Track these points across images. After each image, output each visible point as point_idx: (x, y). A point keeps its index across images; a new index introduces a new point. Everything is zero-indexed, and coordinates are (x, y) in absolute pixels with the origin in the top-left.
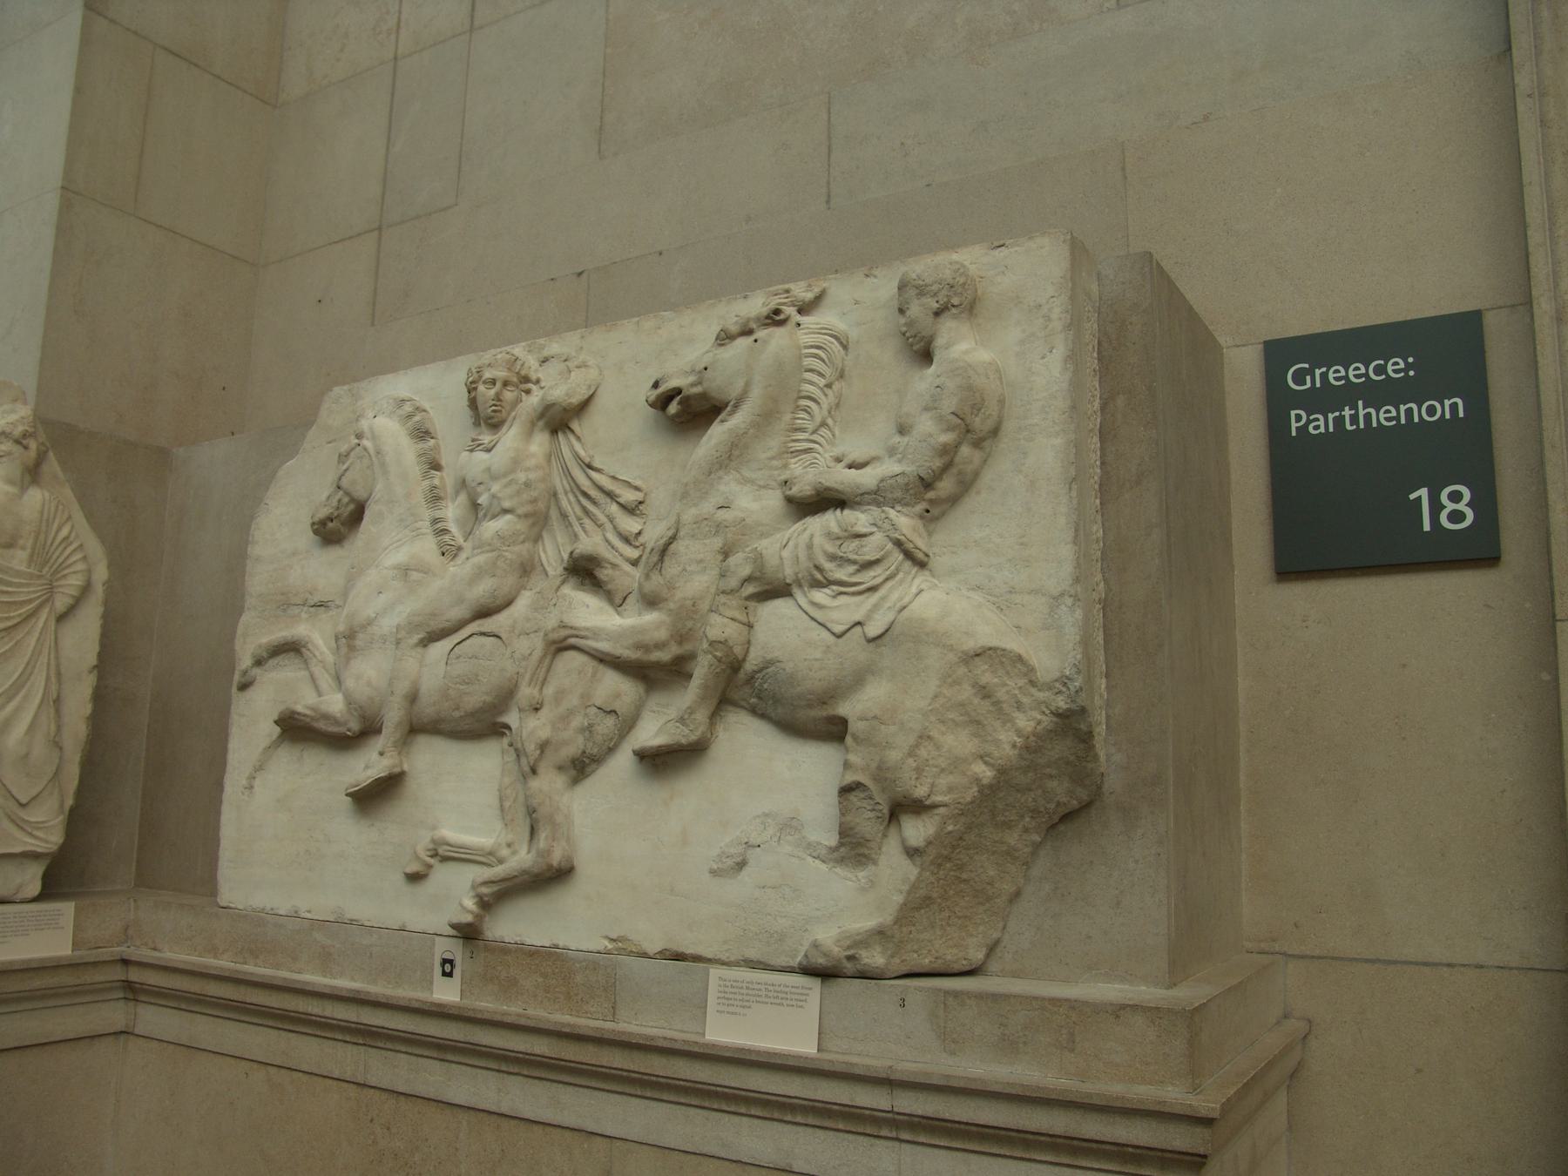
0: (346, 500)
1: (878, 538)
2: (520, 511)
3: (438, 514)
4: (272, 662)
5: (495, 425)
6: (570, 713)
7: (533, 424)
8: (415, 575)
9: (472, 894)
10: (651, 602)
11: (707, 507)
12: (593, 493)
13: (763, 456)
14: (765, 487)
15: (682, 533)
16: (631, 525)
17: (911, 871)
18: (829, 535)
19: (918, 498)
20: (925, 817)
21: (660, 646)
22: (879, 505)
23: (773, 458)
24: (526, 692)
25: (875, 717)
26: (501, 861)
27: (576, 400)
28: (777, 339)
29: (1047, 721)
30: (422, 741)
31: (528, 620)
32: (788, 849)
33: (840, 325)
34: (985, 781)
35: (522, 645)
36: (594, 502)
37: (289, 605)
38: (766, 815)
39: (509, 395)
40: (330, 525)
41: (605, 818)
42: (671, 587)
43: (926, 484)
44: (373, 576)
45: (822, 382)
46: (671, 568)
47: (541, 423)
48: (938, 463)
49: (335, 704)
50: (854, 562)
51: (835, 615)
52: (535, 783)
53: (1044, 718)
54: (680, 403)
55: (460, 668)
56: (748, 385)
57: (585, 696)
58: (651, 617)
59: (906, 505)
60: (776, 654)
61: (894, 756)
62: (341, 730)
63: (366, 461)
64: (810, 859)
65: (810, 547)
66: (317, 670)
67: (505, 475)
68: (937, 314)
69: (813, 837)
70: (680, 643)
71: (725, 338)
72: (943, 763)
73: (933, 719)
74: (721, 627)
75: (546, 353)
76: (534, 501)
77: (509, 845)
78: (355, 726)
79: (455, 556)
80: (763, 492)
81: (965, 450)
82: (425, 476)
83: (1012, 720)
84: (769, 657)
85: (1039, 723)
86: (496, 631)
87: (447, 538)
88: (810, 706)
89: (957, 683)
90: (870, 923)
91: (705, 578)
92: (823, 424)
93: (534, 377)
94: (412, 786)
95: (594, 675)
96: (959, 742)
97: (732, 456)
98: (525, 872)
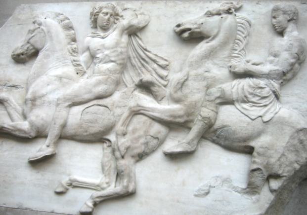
0: (31, 48)
1: (267, 89)
2: (118, 62)
3: (75, 58)
5: (105, 29)
6: (140, 137)
8: (65, 80)
9: (91, 201)
10: (177, 101)
11: (201, 71)
12: (147, 59)
13: (222, 56)
14: (223, 67)
15: (190, 79)
16: (164, 73)
19: (281, 78)
20: (278, 180)
21: (180, 117)
22: (268, 78)
23: (225, 58)
24: (119, 127)
25: (266, 147)
26: (103, 189)
27: (141, 25)
28: (229, 19)
31: (120, 102)
32: (225, 188)
33: (249, 18)
34: (297, 169)
35: (118, 111)
36: (147, 62)
38: (218, 177)
39: (112, 20)
40: (22, 56)
41: (151, 175)
42: (186, 96)
43: (284, 74)
44: (44, 78)
46: (186, 91)
48: (289, 68)
49: (25, 125)
50: (259, 96)
51: (251, 113)
52: (122, 162)
54: (189, 34)
55: (87, 117)
57: (146, 133)
58: (175, 107)
59: (277, 80)
60: (227, 124)
61: (273, 160)
63: (42, 34)
64: (234, 192)
65: (243, 89)
66: (12, 112)
67: (112, 48)
68: (289, 21)
69: (236, 185)
71: (210, 14)
72: (287, 163)
74: (206, 112)
75: (126, 6)
76: (123, 59)
77: (107, 183)
78: (33, 134)
79: (83, 75)
80: (222, 68)
81: (297, 65)
82: (69, 43)
84: (225, 124)
86: (106, 105)
87: (80, 68)
88: (240, 142)
89: (294, 138)
91: (199, 95)
92: (243, 49)
93: (121, 15)
94: (59, 158)
95: (150, 124)
96: (291, 157)
97: (210, 55)
98: (116, 193)
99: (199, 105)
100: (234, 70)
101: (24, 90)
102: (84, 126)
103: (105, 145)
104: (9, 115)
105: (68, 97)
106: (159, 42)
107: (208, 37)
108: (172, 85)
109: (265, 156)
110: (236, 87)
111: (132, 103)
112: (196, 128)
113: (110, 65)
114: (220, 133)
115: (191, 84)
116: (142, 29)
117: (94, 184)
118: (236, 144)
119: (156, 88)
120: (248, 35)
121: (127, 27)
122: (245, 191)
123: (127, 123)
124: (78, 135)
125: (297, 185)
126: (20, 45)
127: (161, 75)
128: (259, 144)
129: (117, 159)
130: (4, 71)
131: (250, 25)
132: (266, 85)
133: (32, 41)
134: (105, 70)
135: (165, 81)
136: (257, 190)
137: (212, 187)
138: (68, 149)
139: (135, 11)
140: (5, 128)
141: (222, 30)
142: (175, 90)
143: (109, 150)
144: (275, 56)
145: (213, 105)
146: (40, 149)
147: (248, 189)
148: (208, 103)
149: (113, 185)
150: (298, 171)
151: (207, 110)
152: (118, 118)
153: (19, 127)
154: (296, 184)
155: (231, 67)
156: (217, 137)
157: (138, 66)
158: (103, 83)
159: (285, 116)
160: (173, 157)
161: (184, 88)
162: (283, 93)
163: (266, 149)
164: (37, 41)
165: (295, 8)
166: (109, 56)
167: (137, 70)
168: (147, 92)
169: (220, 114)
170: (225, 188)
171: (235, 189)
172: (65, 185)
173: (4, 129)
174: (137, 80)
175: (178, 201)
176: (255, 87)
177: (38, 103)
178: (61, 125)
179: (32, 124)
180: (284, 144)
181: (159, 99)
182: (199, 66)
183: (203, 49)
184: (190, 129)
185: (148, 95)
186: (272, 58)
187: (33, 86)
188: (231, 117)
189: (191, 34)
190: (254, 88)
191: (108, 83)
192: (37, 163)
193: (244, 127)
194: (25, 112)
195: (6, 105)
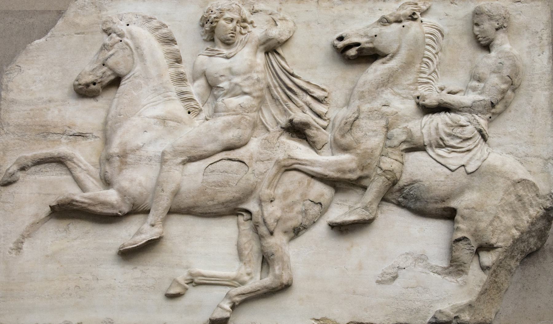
0: (109, 73)
1: (470, 128)
2: (255, 94)
3: (184, 89)
4: (33, 169)
7: (258, 48)
8: (171, 123)
10: (345, 149)
11: (376, 104)
13: (405, 83)
15: (362, 116)
16: (320, 108)
17: (484, 277)
18: (447, 124)
19: (488, 111)
20: (492, 252)
21: (350, 171)
22: (470, 112)
23: (410, 85)
25: (473, 208)
26: (243, 283)
27: (284, 38)
28: (414, 27)
29: (542, 212)
30: (175, 218)
31: (261, 154)
32: (420, 269)
34: (516, 237)
35: (260, 167)
37: (48, 134)
38: (408, 254)
40: (92, 87)
42: (358, 142)
43: (493, 105)
44: (136, 120)
45: (434, 52)
46: (358, 134)
47: (262, 47)
48: (499, 97)
49: (112, 196)
50: (460, 138)
51: (450, 161)
53: (540, 210)
54: (358, 50)
55: (214, 178)
56: (399, 47)
57: (304, 196)
58: (344, 157)
59: (483, 114)
60: (418, 178)
61: (483, 225)
62: (115, 211)
64: (432, 274)
65: (437, 129)
66: (82, 176)
67: (244, 73)
68: (497, 29)
69: (434, 263)
70: (362, 170)
71: (385, 21)
72: (502, 228)
73: (500, 209)
74: (388, 163)
75: (257, 8)
76: (261, 90)
77: (249, 274)
78: (126, 209)
79: (198, 114)
80: (405, 100)
81: (509, 92)
82: (171, 66)
83: (528, 211)
84: (414, 179)
85: (538, 213)
86: (240, 159)
87: (192, 103)
88: (436, 203)
89: (510, 194)
90: (465, 301)
91: (377, 139)
94: (167, 244)
95: (309, 184)
96: (508, 219)
97: (389, 81)
98: (266, 287)
99: (377, 153)
100: (423, 102)
101: (98, 143)
102: (209, 191)
103: (241, 219)
104: (77, 181)
105: (180, 149)
106: (309, 62)
108: (337, 124)
109: (472, 220)
111: (280, 155)
112: (376, 186)
113: (243, 100)
114: (409, 192)
115: (363, 124)
116: (283, 43)
117: (228, 277)
118: (432, 206)
119: (313, 132)
120: (441, 50)
121: (263, 41)
122: (447, 271)
124: (198, 207)
125: (518, 263)
126: (88, 68)
127: (318, 113)
128: (463, 204)
129: (261, 237)
130: (60, 111)
132: (469, 122)
134: (236, 107)
136: (463, 268)
137: (402, 269)
138: (180, 229)
139: (270, 14)
140: (77, 201)
141: (404, 45)
142: (342, 133)
143: (247, 227)
144: (479, 80)
146: (130, 233)
147: (451, 268)
148: (390, 150)
150: (518, 240)
151: (388, 160)
152: (261, 177)
153: (102, 198)
154: (517, 261)
155: (418, 97)
156: (404, 197)
157: (282, 98)
158: (234, 126)
159: (496, 164)
160: (342, 229)
161: (354, 129)
162: (490, 132)
163: (473, 210)
164: (118, 61)
165: (506, 11)
166: (241, 86)
167: (281, 104)
168: (299, 137)
169: (406, 164)
170: (420, 269)
171: (432, 268)
172: (183, 282)
173: (74, 203)
174: (283, 121)
175: (354, 293)
176: (453, 124)
177: (131, 160)
178: (172, 193)
179: (123, 193)
181: (319, 146)
182: (374, 99)
183: (378, 73)
184: (365, 188)
185: (301, 142)
186: (475, 83)
187: (119, 133)
188: (420, 168)
190: (452, 126)
191: (242, 127)
192: (128, 254)
193: (442, 181)
194: (109, 174)
195: (70, 167)
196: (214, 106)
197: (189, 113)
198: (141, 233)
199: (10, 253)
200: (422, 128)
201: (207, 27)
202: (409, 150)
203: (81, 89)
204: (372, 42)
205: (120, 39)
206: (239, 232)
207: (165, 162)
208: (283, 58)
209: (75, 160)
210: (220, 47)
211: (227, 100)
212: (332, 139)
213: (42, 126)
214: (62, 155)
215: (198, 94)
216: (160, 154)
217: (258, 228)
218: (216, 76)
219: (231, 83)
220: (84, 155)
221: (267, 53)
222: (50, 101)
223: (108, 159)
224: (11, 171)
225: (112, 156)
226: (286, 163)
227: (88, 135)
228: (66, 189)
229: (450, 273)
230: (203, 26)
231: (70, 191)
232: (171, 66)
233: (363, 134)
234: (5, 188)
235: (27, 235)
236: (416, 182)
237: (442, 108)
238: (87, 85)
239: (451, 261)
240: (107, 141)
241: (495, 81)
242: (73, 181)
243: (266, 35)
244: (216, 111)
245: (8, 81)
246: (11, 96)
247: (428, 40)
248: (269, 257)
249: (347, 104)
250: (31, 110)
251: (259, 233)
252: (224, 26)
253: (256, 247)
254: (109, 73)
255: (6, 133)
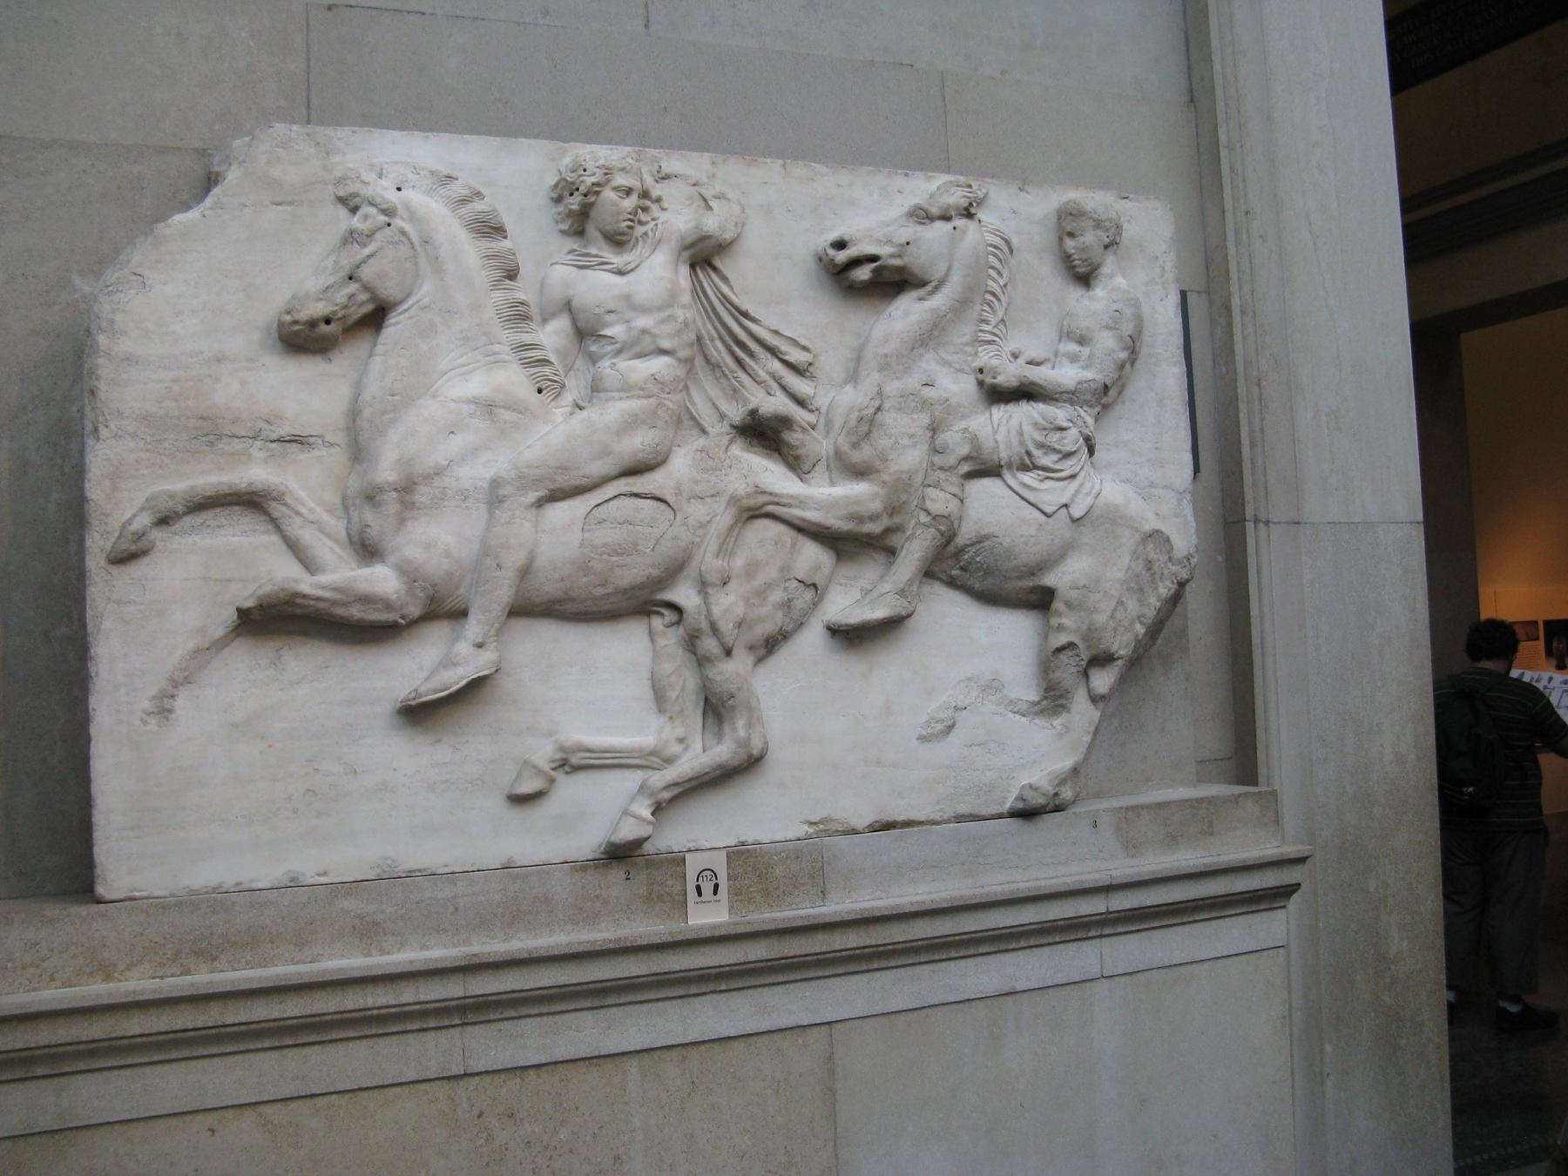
0: (363, 297)
3: (527, 338)
6: (768, 586)
8: (506, 415)
10: (860, 472)
11: (912, 382)
14: (961, 370)
15: (886, 405)
17: (1094, 714)
20: (1108, 669)
21: (873, 518)
22: (1072, 403)
23: (966, 344)
26: (670, 761)
30: (520, 624)
31: (697, 482)
33: (1008, 229)
35: (697, 511)
36: (751, 355)
37: (220, 437)
38: (969, 679)
40: (324, 328)
41: (797, 697)
42: (884, 458)
44: (429, 408)
46: (884, 442)
49: (382, 580)
50: (1059, 452)
55: (605, 536)
56: (950, 268)
57: (785, 569)
58: (860, 488)
61: (1101, 618)
65: (1021, 434)
66: (307, 536)
67: (660, 309)
68: (1106, 247)
69: (1013, 696)
70: (891, 516)
74: (939, 501)
77: (681, 740)
78: (414, 611)
80: (960, 375)
81: (1128, 366)
82: (496, 285)
84: (985, 531)
86: (657, 493)
87: (547, 370)
88: (1020, 578)
90: (1067, 763)
93: (655, 194)
95: (794, 545)
96: (1132, 605)
97: (931, 335)
98: (720, 766)
99: (919, 479)
101: (337, 458)
102: (595, 565)
103: (657, 622)
104: (294, 547)
107: (922, 284)
108: (838, 421)
110: (1002, 429)
112: (915, 550)
113: (659, 365)
114: (972, 558)
116: (723, 248)
117: (641, 750)
119: (795, 436)
121: (690, 240)
123: (726, 547)
124: (571, 600)
126: (313, 285)
127: (799, 395)
129: (702, 661)
130: (244, 383)
131: (1011, 252)
133: (366, 273)
135: (811, 411)
140: (305, 596)
141: (956, 265)
142: (854, 440)
143: (671, 640)
144: (1082, 341)
145: (955, 479)
148: (942, 475)
149: (697, 745)
151: (942, 495)
152: (700, 532)
153: (363, 588)
155: (981, 371)
156: (962, 568)
164: (384, 271)
166: (654, 336)
168: (765, 447)
171: (1013, 706)
173: (299, 601)
174: (736, 414)
175: (879, 763)
177: (423, 499)
179: (410, 574)
180: (1121, 575)
181: (806, 467)
183: (913, 318)
184: (892, 552)
185: (769, 456)
186: (1072, 347)
187: (394, 435)
188: (993, 510)
189: (876, 271)
194: (373, 532)
195: (276, 514)
196: (589, 377)
197: (540, 391)
198: (455, 665)
199: (144, 722)
200: (995, 432)
201: (574, 203)
202: (970, 476)
203: (297, 333)
204: (900, 256)
205: (386, 219)
206: (655, 651)
207: (501, 502)
208: (725, 279)
209: (288, 500)
210: (600, 249)
211: (624, 364)
212: (831, 452)
213: (203, 418)
214: (258, 487)
215: (557, 351)
216: (485, 485)
217: (699, 642)
218: (597, 311)
219: (630, 329)
220: (308, 485)
221: (693, 267)
222: (218, 360)
223: (371, 497)
224: (136, 526)
225: (381, 490)
226: (752, 502)
227: (312, 440)
228: (263, 565)
229: (1042, 711)
230: (558, 200)
231: (277, 572)
232: (496, 285)
233: (892, 441)
234: (122, 568)
235: (183, 679)
236: (986, 537)
237: (1025, 393)
238: (312, 324)
239: (1047, 690)
240: (358, 453)
241: (1106, 342)
242: (284, 547)
243: (697, 227)
244: (596, 388)
245: (114, 311)
246: (124, 345)
247: (991, 259)
248: (723, 703)
249: (853, 377)
250: (175, 380)
251: (700, 651)
252: (615, 204)
253: (690, 681)
254: (363, 297)
255: (115, 436)
